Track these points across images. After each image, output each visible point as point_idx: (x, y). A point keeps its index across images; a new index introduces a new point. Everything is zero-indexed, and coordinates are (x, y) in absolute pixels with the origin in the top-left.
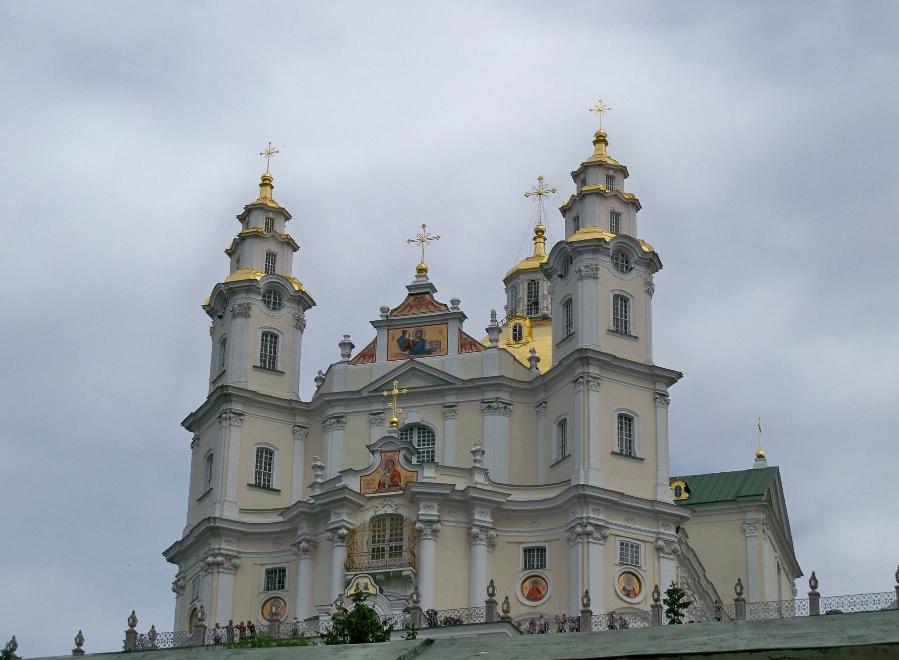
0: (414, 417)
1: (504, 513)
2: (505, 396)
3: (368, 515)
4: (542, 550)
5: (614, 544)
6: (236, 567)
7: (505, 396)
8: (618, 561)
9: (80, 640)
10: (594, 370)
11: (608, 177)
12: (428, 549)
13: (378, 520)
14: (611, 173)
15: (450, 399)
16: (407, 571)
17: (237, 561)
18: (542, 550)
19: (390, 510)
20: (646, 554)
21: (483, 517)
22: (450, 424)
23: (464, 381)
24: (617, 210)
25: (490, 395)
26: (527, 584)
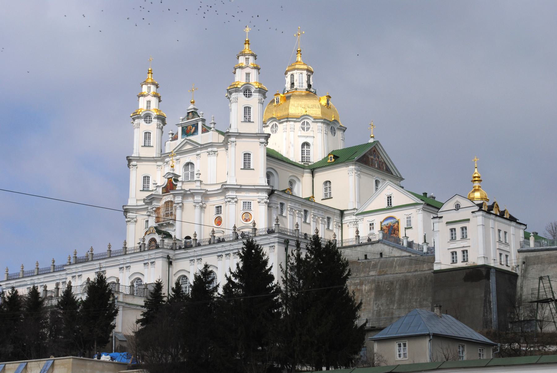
0: (188, 161)
1: (206, 195)
2: (215, 149)
3: (162, 203)
4: (221, 207)
5: (241, 203)
6: (136, 222)
7: (215, 149)
8: (242, 209)
9: (54, 262)
10: (233, 139)
11: (246, 58)
12: (178, 213)
13: (167, 203)
14: (247, 57)
15: (198, 152)
16: (171, 222)
17: (135, 219)
18: (221, 207)
19: (169, 199)
20: (254, 205)
21: (198, 199)
22: (198, 161)
23: (201, 145)
24: (248, 72)
25: (210, 149)
26: (217, 220)
